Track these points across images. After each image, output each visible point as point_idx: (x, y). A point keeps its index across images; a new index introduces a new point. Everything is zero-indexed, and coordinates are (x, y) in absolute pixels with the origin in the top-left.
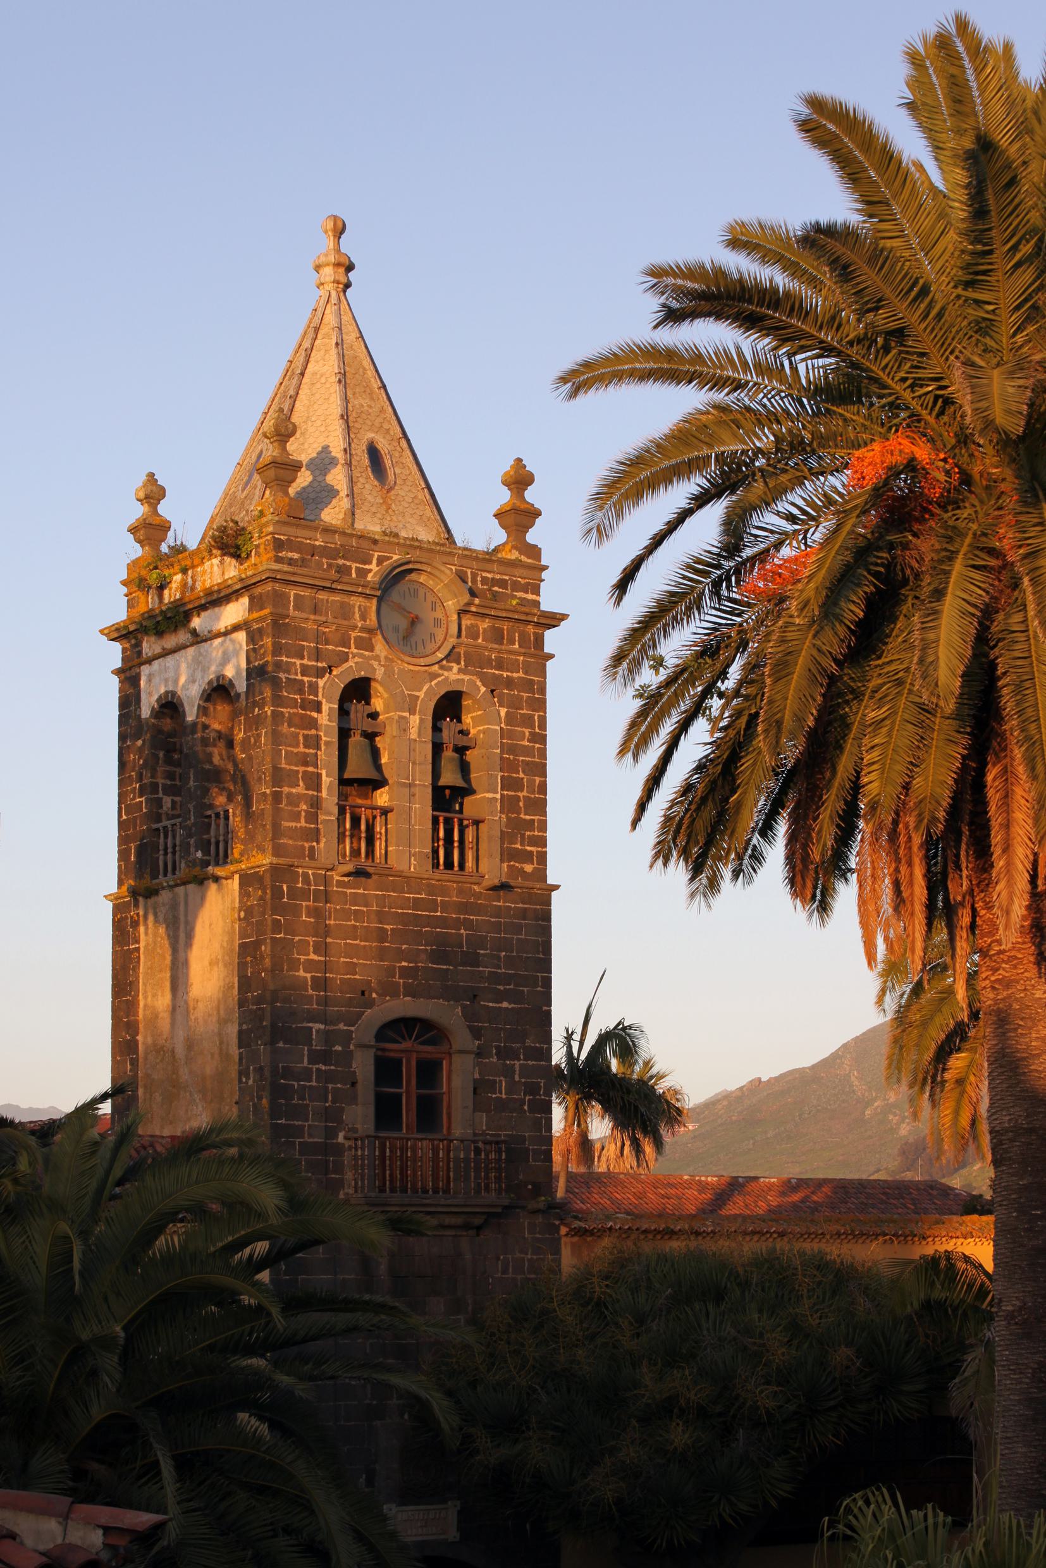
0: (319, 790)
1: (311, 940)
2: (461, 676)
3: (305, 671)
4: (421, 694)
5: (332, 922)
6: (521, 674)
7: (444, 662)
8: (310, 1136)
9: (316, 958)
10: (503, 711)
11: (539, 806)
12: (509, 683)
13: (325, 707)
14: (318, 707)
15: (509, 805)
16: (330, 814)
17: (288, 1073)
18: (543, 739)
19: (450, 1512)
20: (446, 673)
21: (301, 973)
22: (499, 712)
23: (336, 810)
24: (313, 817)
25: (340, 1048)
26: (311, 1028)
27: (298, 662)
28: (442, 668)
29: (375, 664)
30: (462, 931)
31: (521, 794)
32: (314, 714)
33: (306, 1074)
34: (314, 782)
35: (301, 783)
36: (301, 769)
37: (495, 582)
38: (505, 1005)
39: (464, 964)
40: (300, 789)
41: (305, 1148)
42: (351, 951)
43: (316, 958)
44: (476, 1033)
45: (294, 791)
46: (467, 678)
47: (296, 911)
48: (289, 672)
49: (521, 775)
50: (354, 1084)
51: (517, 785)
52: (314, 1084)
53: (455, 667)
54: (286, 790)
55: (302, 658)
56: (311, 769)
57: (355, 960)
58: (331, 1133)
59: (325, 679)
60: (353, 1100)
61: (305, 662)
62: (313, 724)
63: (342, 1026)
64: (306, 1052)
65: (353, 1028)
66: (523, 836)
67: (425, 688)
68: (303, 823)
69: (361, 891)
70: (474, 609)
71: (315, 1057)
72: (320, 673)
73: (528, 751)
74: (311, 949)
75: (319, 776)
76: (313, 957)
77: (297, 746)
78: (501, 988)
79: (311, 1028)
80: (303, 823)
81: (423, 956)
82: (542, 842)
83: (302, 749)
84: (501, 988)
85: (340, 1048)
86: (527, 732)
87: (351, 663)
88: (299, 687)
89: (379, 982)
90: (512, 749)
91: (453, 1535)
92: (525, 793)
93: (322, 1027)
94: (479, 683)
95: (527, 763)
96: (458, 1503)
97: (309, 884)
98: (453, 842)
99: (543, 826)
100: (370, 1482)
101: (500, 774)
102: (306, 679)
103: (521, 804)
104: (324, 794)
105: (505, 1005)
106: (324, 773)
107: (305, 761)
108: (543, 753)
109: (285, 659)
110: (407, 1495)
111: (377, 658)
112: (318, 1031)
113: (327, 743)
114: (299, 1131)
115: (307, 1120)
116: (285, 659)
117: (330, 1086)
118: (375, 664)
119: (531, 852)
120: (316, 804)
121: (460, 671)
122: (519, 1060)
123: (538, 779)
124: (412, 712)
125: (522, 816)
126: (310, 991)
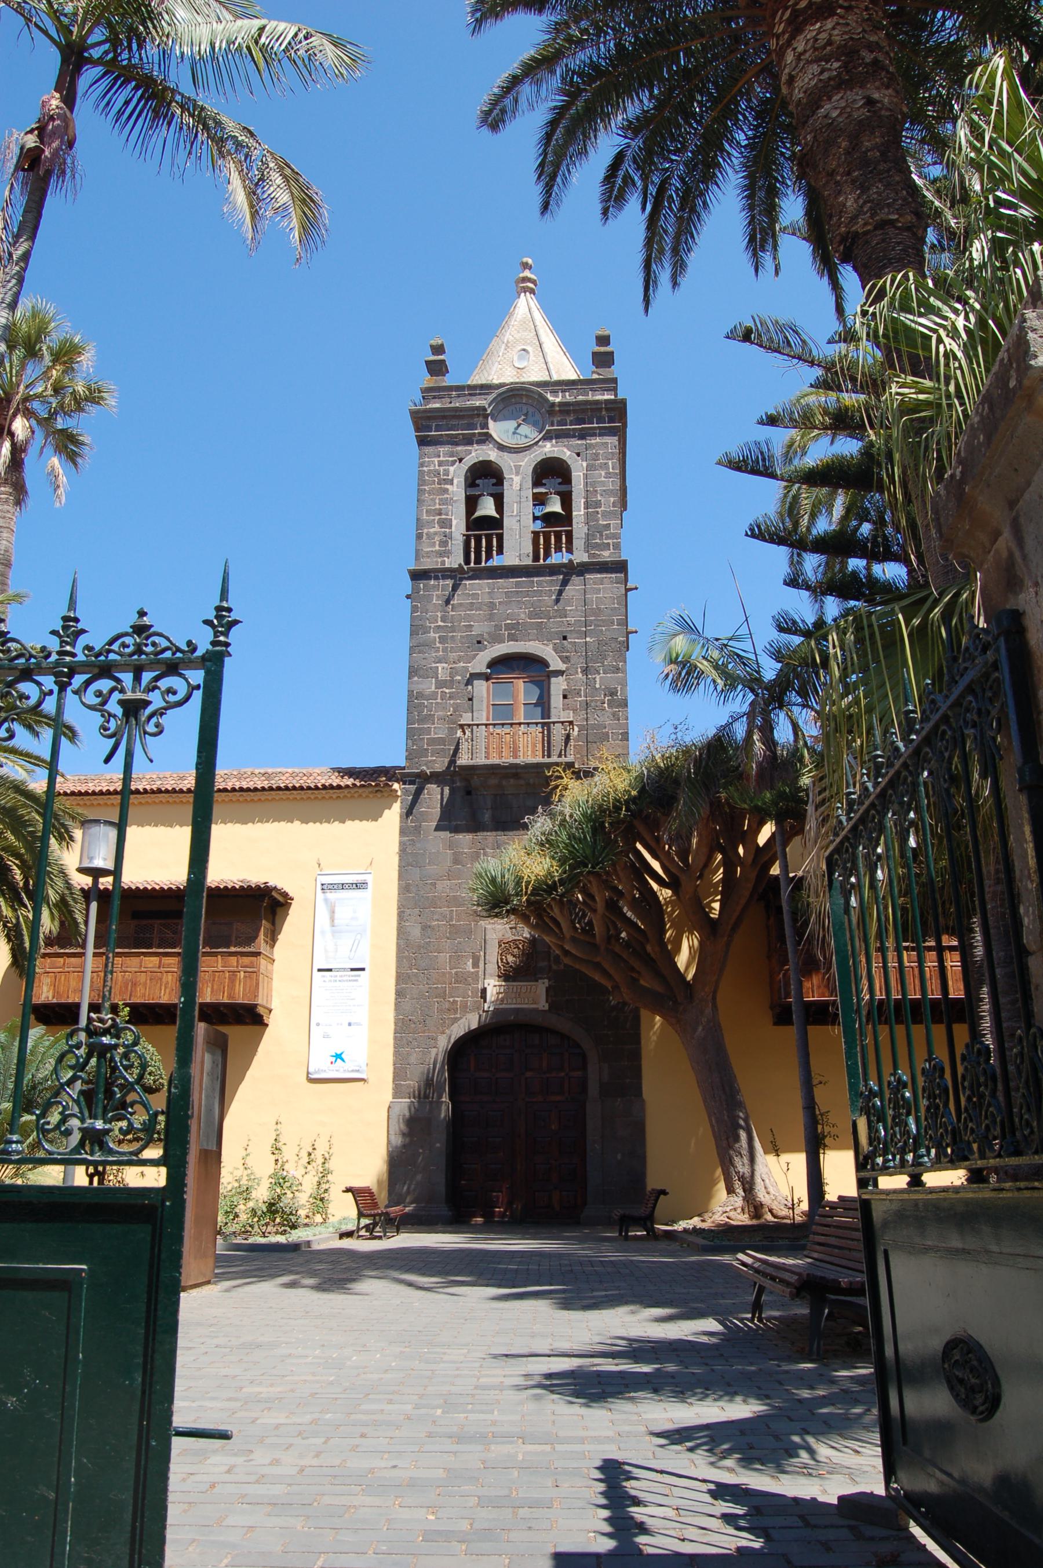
10: (585, 464)
13: (455, 481)
14: (451, 482)
15: (589, 518)
17: (420, 695)
19: (541, 988)
27: (436, 460)
31: (599, 510)
32: (447, 486)
33: (433, 696)
34: (446, 524)
36: (437, 518)
39: (555, 617)
40: (437, 529)
41: (432, 741)
42: (468, 618)
44: (565, 660)
45: (432, 530)
47: (430, 597)
51: (598, 504)
52: (439, 701)
53: (548, 445)
58: (452, 731)
61: (441, 459)
62: (446, 491)
63: (462, 664)
66: (601, 535)
68: (437, 548)
71: (440, 684)
72: (453, 463)
73: (603, 483)
77: (435, 504)
80: (437, 548)
81: (523, 616)
83: (437, 506)
86: (603, 473)
87: (473, 454)
89: (489, 634)
90: (594, 484)
91: (543, 1005)
93: (446, 665)
94: (565, 450)
98: (550, 544)
100: (475, 965)
101: (583, 500)
102: (441, 469)
114: (428, 731)
119: (608, 544)
120: (448, 537)
121: (553, 446)
124: (517, 474)
126: (438, 645)
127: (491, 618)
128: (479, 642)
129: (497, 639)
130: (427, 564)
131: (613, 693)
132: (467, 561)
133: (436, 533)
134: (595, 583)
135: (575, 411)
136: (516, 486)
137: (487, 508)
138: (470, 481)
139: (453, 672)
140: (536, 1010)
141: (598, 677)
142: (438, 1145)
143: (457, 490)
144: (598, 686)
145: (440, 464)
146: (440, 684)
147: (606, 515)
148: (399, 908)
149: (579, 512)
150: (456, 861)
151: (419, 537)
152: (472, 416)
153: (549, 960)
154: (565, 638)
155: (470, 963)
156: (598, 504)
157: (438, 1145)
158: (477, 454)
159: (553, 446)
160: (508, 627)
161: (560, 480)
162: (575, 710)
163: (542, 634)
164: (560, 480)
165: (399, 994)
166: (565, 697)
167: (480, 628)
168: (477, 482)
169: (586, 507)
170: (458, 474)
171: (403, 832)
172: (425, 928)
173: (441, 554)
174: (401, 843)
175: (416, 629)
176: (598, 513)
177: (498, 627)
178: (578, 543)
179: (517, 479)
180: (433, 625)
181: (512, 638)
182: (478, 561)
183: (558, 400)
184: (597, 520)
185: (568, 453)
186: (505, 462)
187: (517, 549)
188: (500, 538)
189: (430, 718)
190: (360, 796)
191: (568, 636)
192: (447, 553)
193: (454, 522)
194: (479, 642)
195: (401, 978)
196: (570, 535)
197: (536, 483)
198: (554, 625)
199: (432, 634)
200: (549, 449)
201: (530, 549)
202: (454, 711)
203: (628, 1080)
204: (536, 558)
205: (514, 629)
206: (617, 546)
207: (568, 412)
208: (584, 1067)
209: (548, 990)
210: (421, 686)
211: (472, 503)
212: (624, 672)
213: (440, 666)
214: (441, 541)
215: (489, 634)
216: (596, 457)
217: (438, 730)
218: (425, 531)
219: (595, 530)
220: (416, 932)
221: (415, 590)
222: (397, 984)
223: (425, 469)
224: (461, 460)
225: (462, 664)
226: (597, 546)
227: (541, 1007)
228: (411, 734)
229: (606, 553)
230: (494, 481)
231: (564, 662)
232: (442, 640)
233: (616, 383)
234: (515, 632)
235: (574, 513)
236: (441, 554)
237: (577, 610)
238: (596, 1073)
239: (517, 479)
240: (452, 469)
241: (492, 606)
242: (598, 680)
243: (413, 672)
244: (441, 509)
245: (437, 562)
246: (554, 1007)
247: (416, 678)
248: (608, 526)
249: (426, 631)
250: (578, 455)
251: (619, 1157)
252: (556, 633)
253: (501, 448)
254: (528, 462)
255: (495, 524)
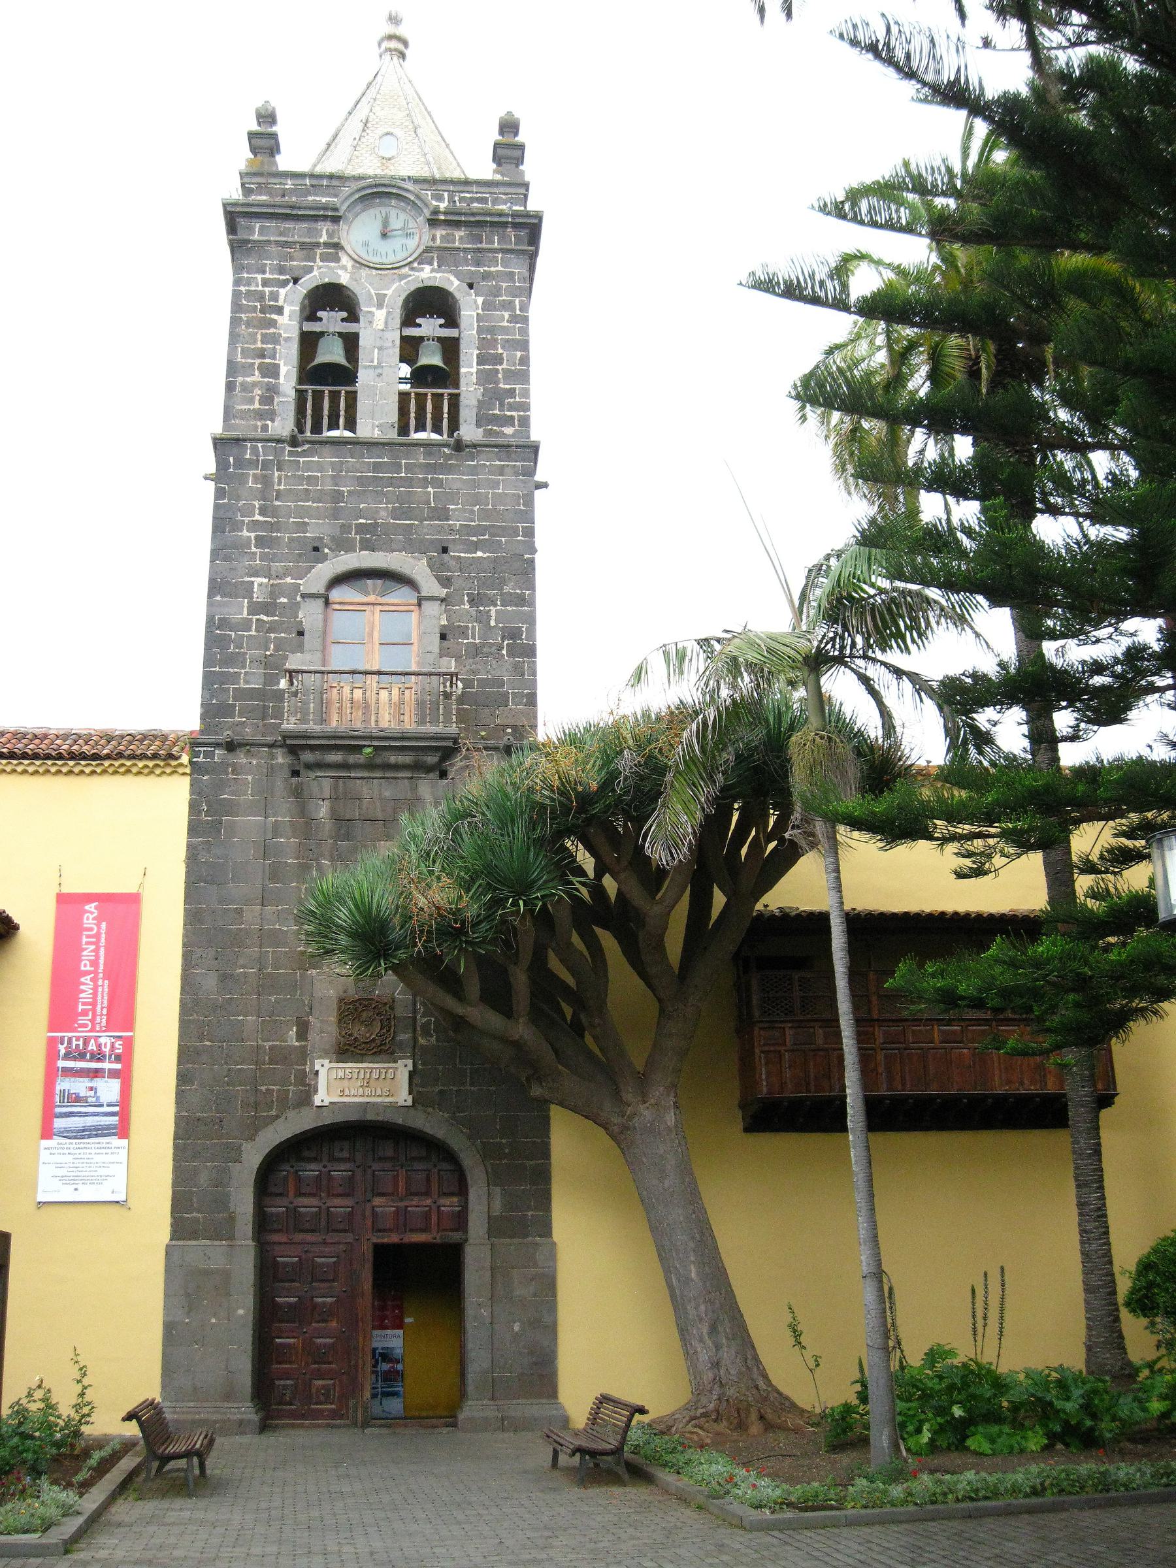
0: (276, 375)
1: (257, 503)
2: (434, 274)
3: (265, 283)
4: (389, 292)
5: (282, 487)
6: (500, 268)
7: (415, 265)
8: (247, 682)
9: (261, 519)
10: (480, 300)
11: (522, 376)
12: (487, 276)
13: (287, 311)
14: (280, 310)
15: (486, 378)
16: (285, 396)
17: (224, 623)
18: (525, 320)
19: (402, 1069)
20: (417, 274)
21: (245, 533)
22: (476, 302)
23: (293, 393)
24: (267, 400)
25: (285, 600)
26: (253, 582)
27: (259, 277)
28: (412, 269)
29: (340, 272)
30: (430, 489)
31: (499, 367)
32: (274, 316)
34: (272, 371)
35: (257, 373)
36: (258, 361)
37: (472, 200)
38: (479, 554)
39: (431, 519)
40: (257, 377)
41: (240, 694)
43: (261, 519)
44: (445, 582)
45: (249, 379)
46: (438, 275)
47: (242, 479)
48: (249, 284)
49: (500, 351)
50: (301, 633)
51: (498, 359)
52: (253, 633)
53: (427, 268)
54: (240, 379)
55: (264, 272)
56: (267, 361)
57: (306, 520)
58: (272, 680)
59: (288, 288)
60: (300, 648)
61: (267, 276)
62: (273, 324)
63: (289, 580)
64: (246, 604)
65: (301, 582)
66: (502, 405)
67: (395, 286)
68: (257, 406)
69: (316, 459)
70: (442, 217)
71: (255, 608)
72: (284, 284)
73: (505, 330)
74: (257, 511)
75: (278, 366)
76: (258, 517)
77: (255, 342)
78: (475, 539)
79: (253, 582)
80: (257, 406)
81: (383, 514)
82: (525, 407)
83: (259, 345)
84: (475, 539)
85: (285, 600)
86: (506, 315)
87: (315, 273)
88: (261, 297)
89: (333, 539)
90: (492, 330)
91: (403, 1097)
92: (505, 366)
93: (265, 580)
94: (452, 278)
95: (507, 341)
96: (410, 1062)
97: (258, 456)
99: (526, 393)
100: (302, 1035)
101: (476, 352)
102: (267, 289)
103: (500, 376)
104: (282, 380)
105: (479, 554)
106: (282, 363)
107: (262, 354)
108: (524, 331)
109: (246, 275)
110: (346, 1051)
111: (344, 268)
112: (260, 585)
113: (287, 339)
115: (244, 667)
116: (246, 275)
117: (273, 635)
118: (340, 272)
119: (512, 417)
121: (432, 271)
122: (496, 605)
123: (519, 354)
124: (380, 306)
125: (501, 385)
126: (254, 549)
127: (335, 514)
128: (316, 549)
129: (342, 545)
130: (242, 427)
131: (514, 634)
132: (300, 426)
133: (255, 384)
134: (491, 473)
135: (467, 224)
136: (379, 323)
137: (331, 353)
138: (307, 312)
139: (274, 591)
140: (394, 1107)
141: (493, 610)
142: (241, 1312)
143: (288, 323)
144: (493, 623)
145: (265, 283)
146: (255, 608)
147: (510, 375)
148: (184, 945)
149: (469, 369)
150: (275, 876)
151: (230, 387)
152: (315, 218)
153: (415, 1031)
154: (445, 550)
155: (293, 1033)
156: (498, 359)
157: (241, 1312)
158: (319, 274)
159: (432, 271)
160: (361, 529)
161: (442, 321)
162: (458, 658)
163: (413, 546)
164: (442, 321)
165: (183, 1078)
166: (443, 637)
167: (318, 528)
168: (319, 314)
169: (480, 362)
170: (291, 300)
171: (193, 830)
172: (224, 978)
173: (260, 415)
174: (190, 846)
175: (223, 523)
176: (497, 371)
177: (345, 528)
178: (467, 414)
179: (380, 315)
180: (246, 520)
181: (368, 546)
182: (317, 429)
183: (443, 206)
184: (497, 382)
185: (456, 283)
186: (363, 286)
187: (376, 415)
188: (352, 398)
189: (235, 659)
190: (128, 771)
191: (451, 547)
192: (272, 415)
193: (283, 370)
194: (316, 549)
195: (184, 1054)
196: (455, 401)
197: (409, 319)
198: (429, 530)
199: (245, 533)
200: (427, 275)
201: (394, 418)
202: (276, 649)
203: (530, 1213)
204: (404, 430)
205: (367, 532)
206: (525, 422)
207: (457, 224)
208: (462, 1190)
209: (412, 1075)
210: (226, 610)
211: (309, 342)
212: (532, 604)
213: (257, 580)
214: (261, 396)
215: (333, 539)
216: (497, 292)
217: (250, 678)
218: (240, 379)
219: (493, 396)
220: (209, 982)
221: (222, 464)
222: (181, 1061)
223: (243, 289)
224: (296, 281)
225: (289, 580)
226: (496, 420)
227: (401, 1103)
228: (209, 680)
229: (508, 430)
230: (344, 314)
231: (444, 586)
232: (260, 542)
233: (527, 190)
234: (372, 538)
235: (463, 370)
236: (260, 415)
237: (463, 510)
238: (482, 1203)
239: (380, 315)
240: (282, 292)
241: (337, 496)
242: (493, 614)
243: (215, 587)
244: (264, 349)
245: (256, 427)
246: (419, 1099)
247: (218, 598)
248: (512, 392)
249: (237, 526)
250: (471, 286)
251: (517, 1327)
252: (432, 542)
253: (360, 264)
254: (396, 292)
255: (344, 375)
